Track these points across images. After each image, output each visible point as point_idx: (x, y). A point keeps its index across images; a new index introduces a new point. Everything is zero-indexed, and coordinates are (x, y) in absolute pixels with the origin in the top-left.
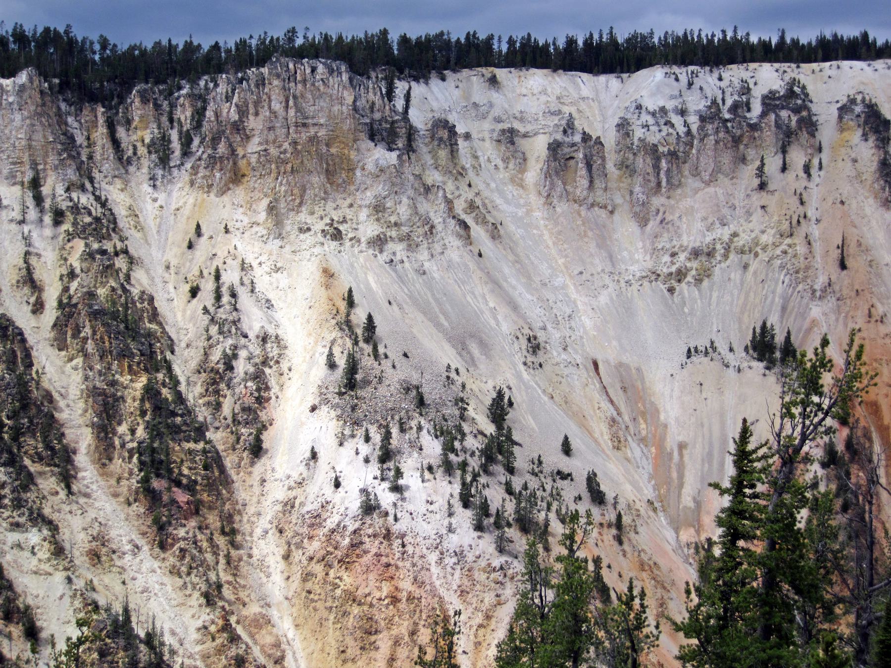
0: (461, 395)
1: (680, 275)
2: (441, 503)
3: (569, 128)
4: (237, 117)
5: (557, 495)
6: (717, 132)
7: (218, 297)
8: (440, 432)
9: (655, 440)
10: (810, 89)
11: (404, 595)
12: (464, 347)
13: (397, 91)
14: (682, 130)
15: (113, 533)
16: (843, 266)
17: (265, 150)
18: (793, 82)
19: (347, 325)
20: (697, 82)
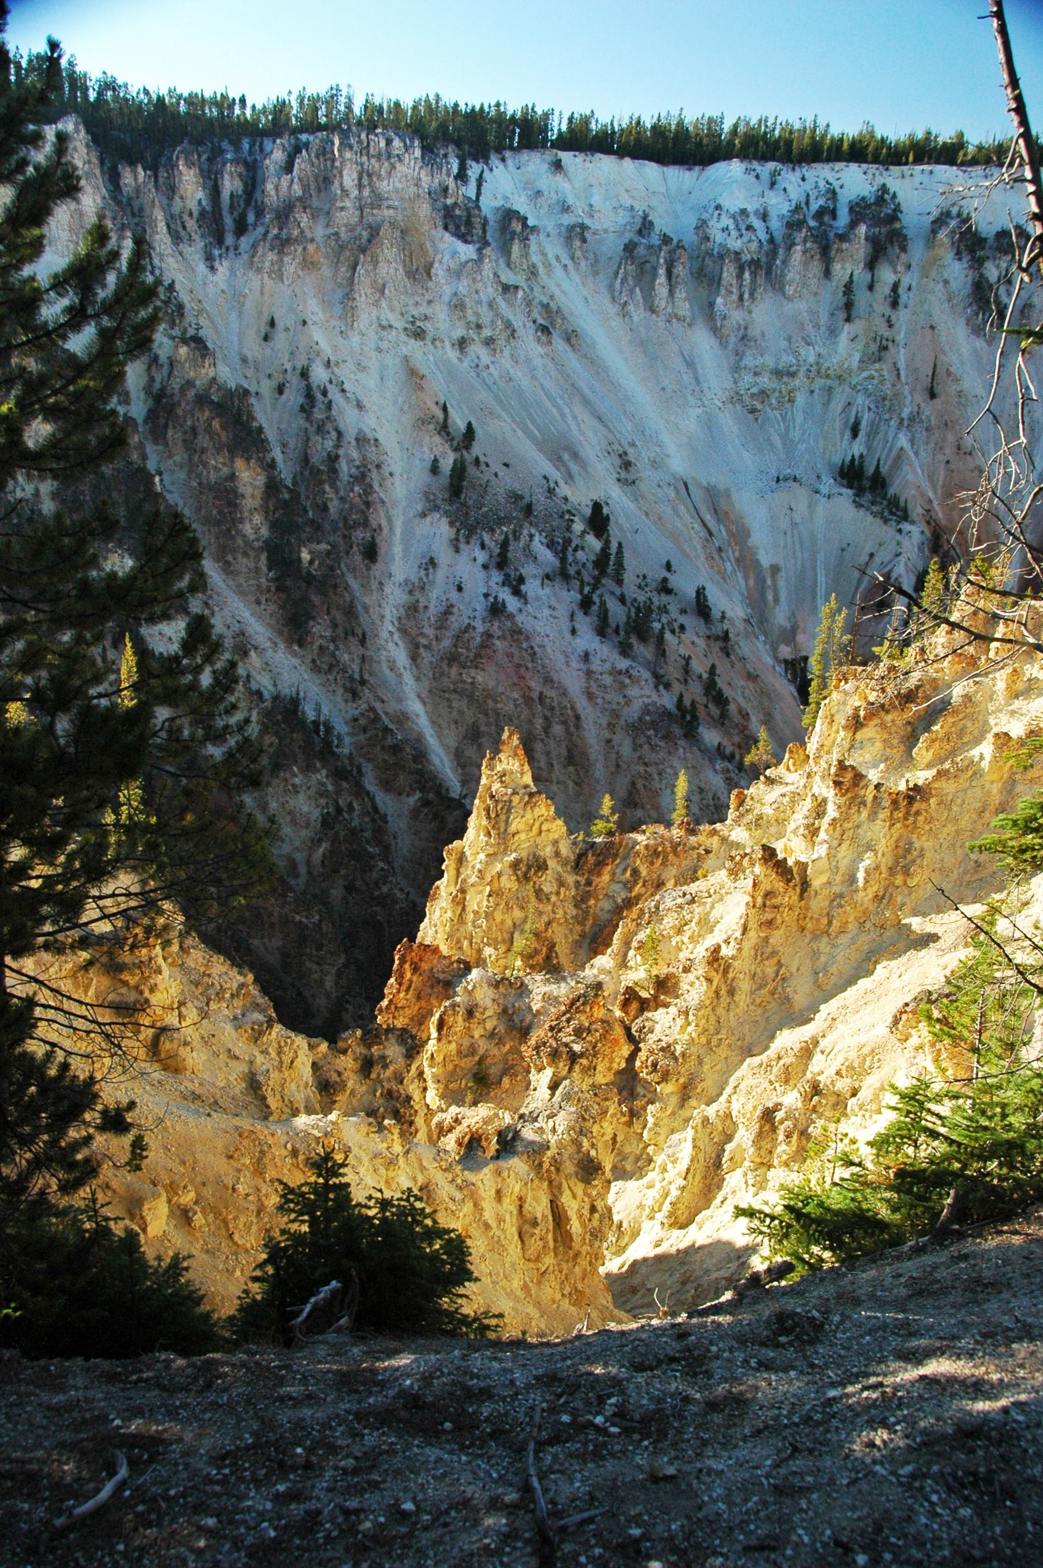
0: (565, 508)
1: (763, 394)
2: (563, 613)
3: (646, 226)
4: (300, 193)
5: (663, 609)
6: (805, 242)
7: (309, 395)
8: (551, 545)
9: (747, 562)
10: (900, 198)
11: (535, 695)
12: (560, 459)
13: (469, 173)
14: (763, 236)
15: (250, 631)
16: (933, 395)
17: (336, 234)
18: (884, 188)
19: (444, 428)
20: (782, 183)
